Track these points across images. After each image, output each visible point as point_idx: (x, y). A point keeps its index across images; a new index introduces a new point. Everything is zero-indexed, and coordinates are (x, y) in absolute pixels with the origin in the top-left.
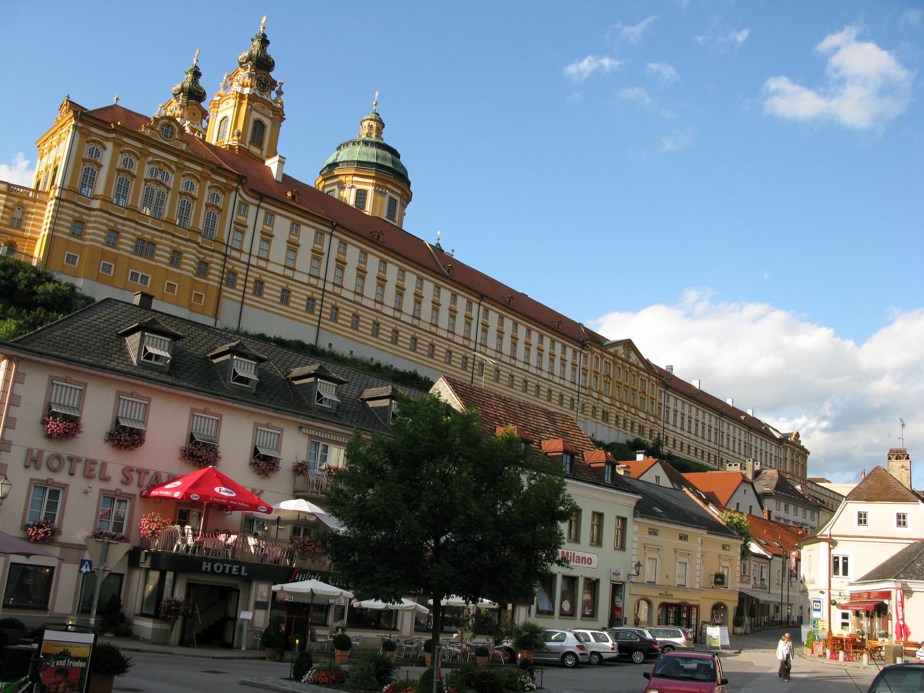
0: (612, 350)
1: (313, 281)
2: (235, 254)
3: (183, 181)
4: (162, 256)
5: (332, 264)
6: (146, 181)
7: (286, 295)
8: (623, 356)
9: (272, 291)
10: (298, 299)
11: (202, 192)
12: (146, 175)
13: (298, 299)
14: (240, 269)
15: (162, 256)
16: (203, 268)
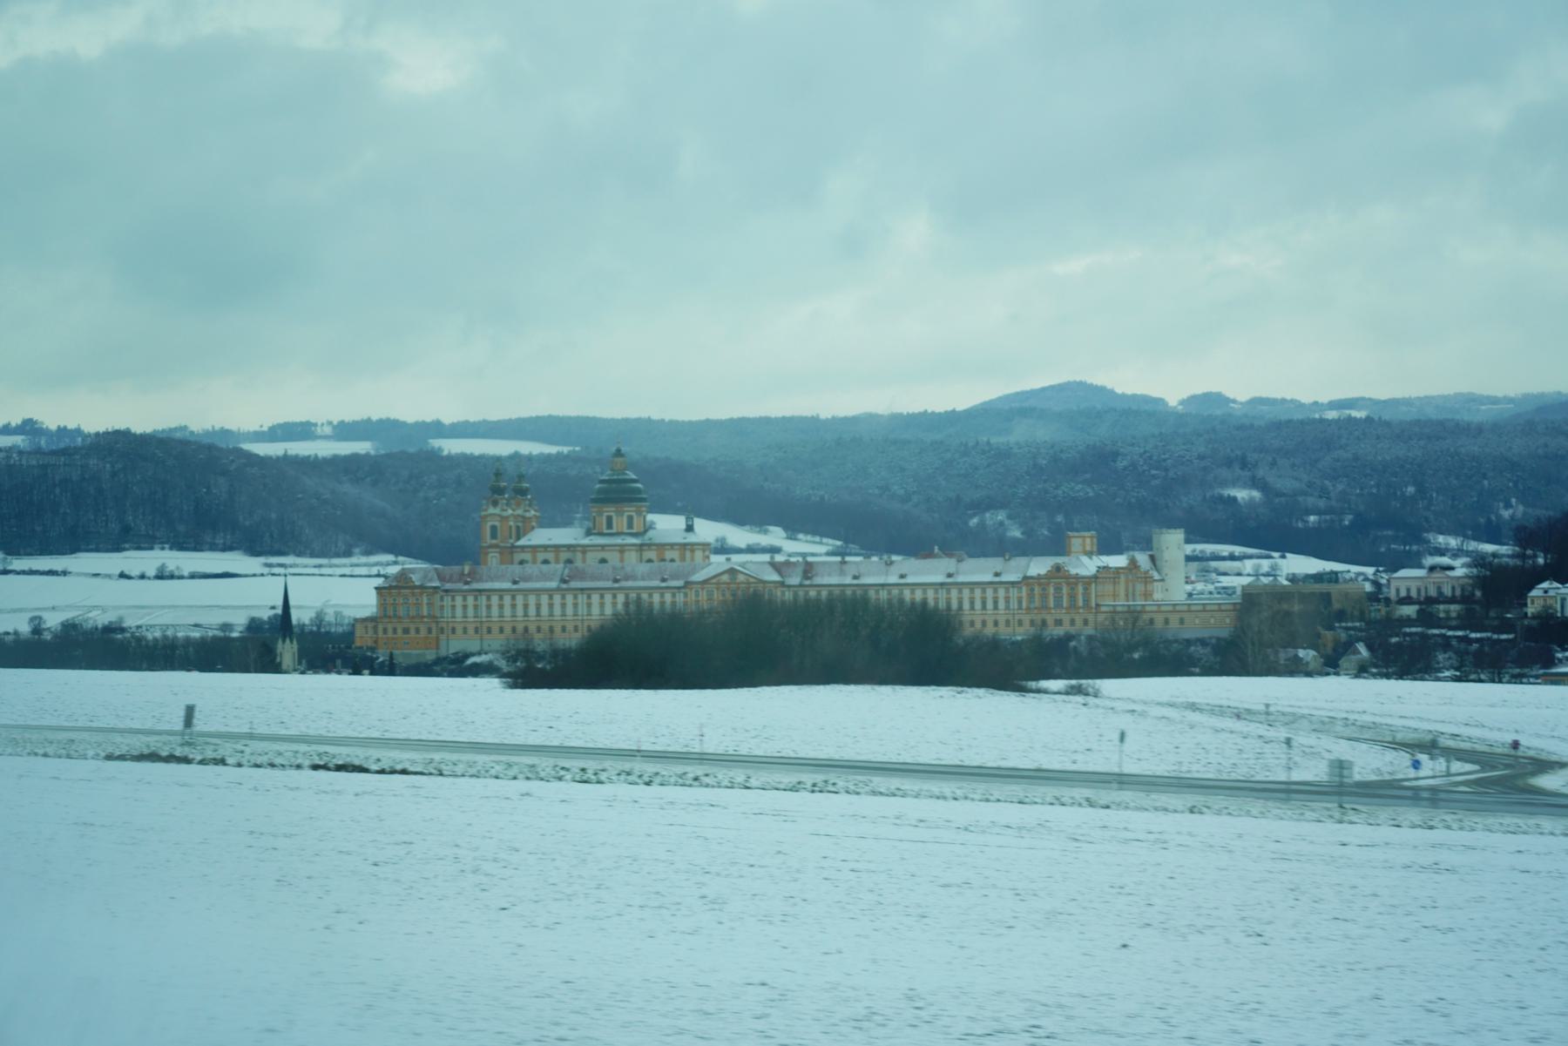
0: (714, 581)
1: (476, 619)
2: (442, 620)
3: (414, 598)
4: (413, 632)
5: (484, 609)
6: (402, 604)
7: (465, 630)
8: (728, 581)
9: (459, 631)
10: (471, 631)
11: (422, 601)
12: (402, 601)
13: (471, 631)
14: (444, 625)
15: (413, 632)
16: (430, 631)
